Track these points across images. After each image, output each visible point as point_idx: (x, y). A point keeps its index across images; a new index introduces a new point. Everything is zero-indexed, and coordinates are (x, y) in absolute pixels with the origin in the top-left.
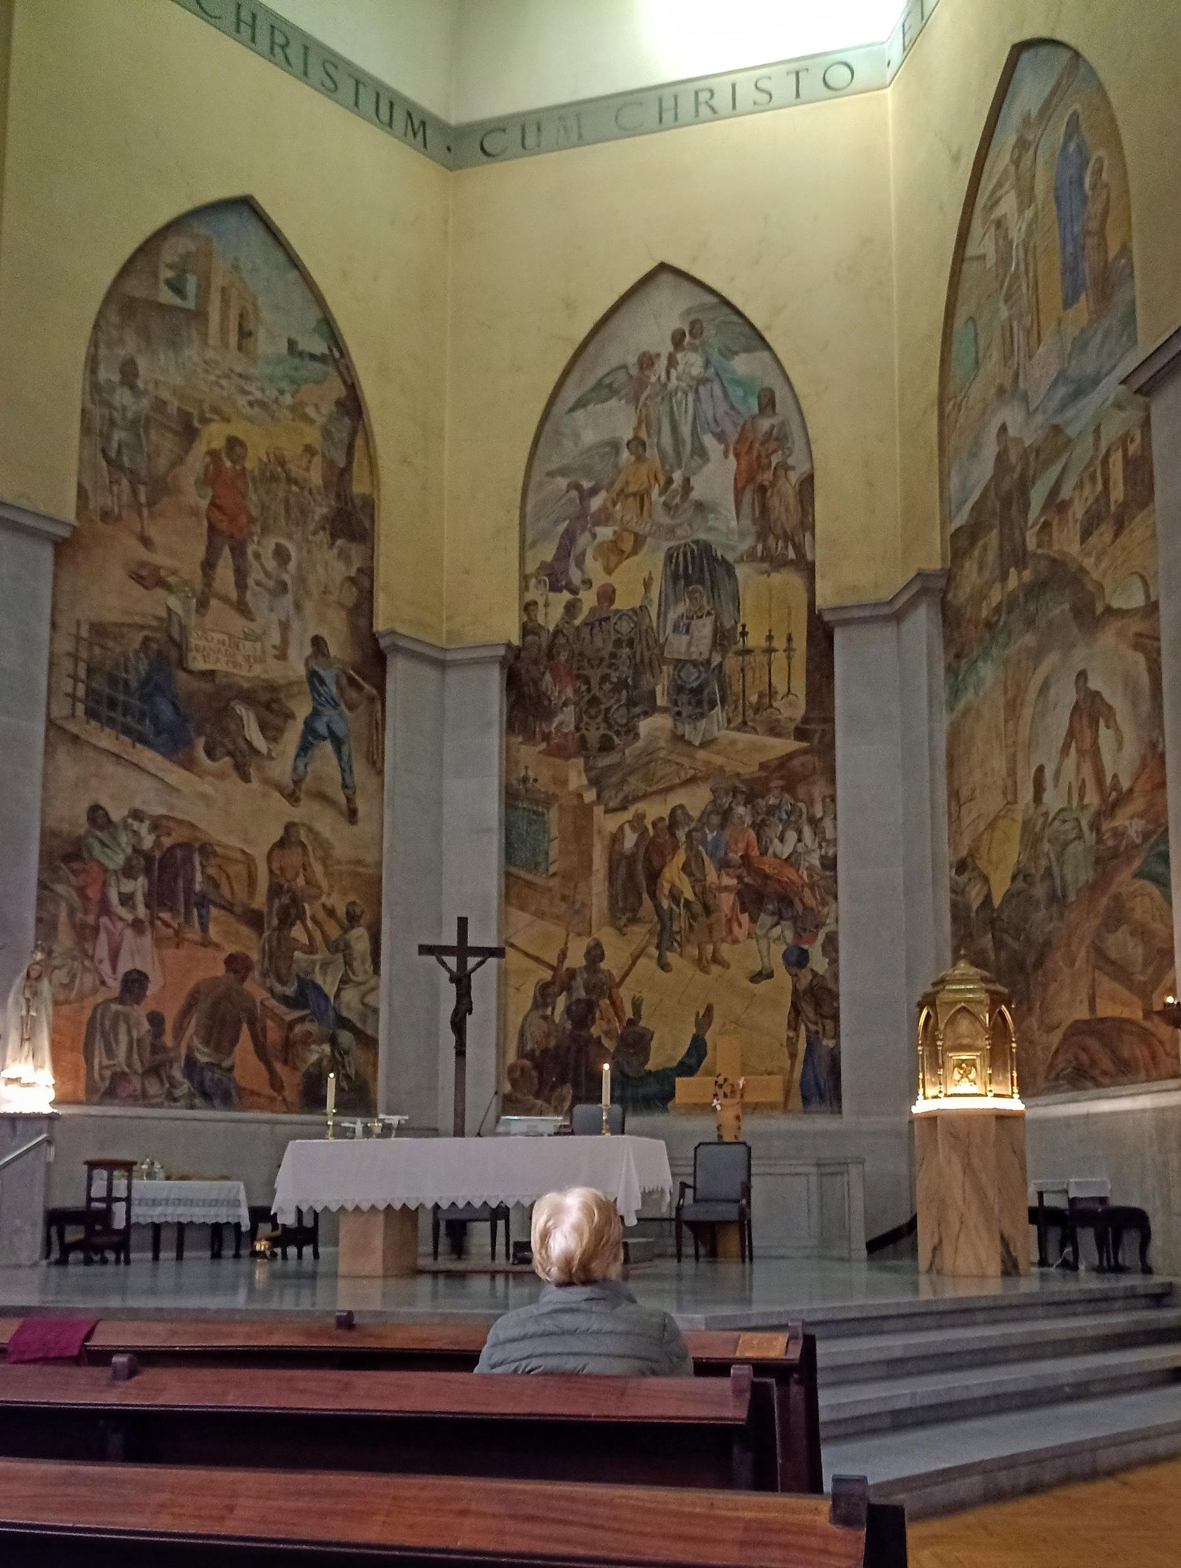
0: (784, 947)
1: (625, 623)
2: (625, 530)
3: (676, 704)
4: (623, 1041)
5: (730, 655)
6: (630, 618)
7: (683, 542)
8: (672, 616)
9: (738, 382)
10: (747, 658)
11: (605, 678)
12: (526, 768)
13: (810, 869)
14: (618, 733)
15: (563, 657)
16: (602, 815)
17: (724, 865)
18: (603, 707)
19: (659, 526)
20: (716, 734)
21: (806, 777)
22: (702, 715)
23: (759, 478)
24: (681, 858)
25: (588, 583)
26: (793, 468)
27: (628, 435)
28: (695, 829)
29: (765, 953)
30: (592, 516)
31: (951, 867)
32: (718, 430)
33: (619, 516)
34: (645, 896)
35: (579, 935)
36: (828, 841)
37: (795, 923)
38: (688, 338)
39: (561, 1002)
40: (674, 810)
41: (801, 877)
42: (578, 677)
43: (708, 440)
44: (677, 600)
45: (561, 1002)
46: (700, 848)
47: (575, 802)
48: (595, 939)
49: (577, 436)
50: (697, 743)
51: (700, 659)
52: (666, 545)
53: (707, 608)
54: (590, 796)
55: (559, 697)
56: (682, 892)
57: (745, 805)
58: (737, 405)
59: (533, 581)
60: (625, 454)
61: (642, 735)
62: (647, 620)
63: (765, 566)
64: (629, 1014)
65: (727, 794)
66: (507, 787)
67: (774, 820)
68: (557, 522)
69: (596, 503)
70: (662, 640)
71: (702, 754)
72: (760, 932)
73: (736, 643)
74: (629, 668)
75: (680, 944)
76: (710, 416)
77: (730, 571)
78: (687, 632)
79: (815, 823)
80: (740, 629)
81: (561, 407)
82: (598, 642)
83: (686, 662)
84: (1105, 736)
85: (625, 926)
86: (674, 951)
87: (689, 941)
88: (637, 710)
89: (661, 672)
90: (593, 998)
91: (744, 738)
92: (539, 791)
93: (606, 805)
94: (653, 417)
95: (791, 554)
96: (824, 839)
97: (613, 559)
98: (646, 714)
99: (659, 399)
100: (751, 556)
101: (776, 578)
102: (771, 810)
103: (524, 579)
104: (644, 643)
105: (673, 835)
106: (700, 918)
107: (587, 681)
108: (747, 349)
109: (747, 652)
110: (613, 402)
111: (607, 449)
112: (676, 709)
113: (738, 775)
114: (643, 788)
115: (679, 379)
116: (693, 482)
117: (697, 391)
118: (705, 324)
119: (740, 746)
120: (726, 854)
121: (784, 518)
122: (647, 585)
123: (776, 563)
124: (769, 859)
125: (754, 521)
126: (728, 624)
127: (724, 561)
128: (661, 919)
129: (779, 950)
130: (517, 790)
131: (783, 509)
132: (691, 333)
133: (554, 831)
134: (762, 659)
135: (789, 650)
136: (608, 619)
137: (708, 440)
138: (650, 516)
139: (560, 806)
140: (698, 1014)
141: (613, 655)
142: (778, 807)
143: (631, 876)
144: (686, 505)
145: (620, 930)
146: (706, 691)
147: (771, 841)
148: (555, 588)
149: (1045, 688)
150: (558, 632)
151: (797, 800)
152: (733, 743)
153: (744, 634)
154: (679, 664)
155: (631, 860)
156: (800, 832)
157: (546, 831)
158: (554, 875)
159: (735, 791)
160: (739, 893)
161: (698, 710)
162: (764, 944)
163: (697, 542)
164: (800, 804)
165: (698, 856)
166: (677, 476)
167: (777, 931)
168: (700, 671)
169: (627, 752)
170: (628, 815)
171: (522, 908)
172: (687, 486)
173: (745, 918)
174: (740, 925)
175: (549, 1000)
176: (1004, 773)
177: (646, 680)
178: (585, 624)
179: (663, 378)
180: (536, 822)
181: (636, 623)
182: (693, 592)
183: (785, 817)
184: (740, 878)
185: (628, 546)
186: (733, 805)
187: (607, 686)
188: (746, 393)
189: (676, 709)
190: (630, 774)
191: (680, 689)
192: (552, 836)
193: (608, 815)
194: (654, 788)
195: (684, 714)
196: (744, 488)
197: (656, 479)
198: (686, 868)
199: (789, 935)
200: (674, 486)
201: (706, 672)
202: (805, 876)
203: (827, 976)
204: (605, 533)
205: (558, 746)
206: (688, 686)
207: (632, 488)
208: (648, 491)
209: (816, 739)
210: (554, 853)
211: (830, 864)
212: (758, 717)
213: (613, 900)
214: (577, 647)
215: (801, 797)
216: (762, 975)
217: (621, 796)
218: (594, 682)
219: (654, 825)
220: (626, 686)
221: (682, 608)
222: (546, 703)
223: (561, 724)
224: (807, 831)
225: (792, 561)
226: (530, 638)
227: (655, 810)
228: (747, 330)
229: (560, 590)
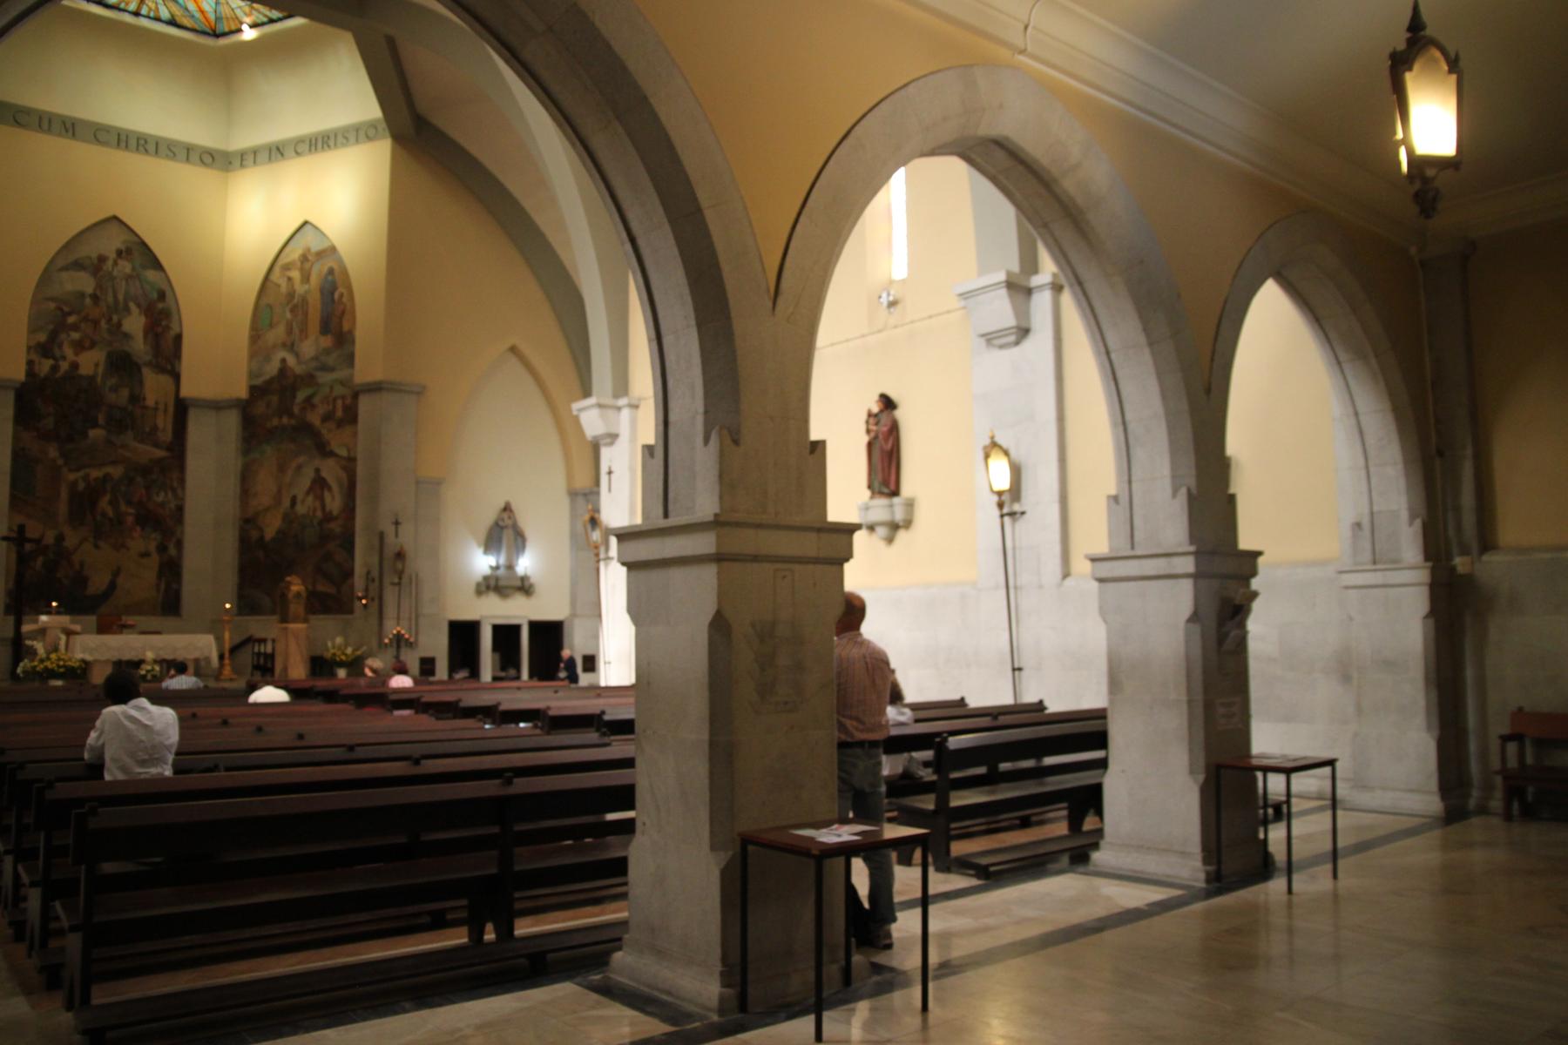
17: (129, 503)
24: (107, 497)
25: (64, 358)
27: (89, 290)
43: (132, 305)
54: (60, 462)
60: (88, 301)
69: (71, 319)
79: (174, 490)
84: (327, 494)
91: (142, 447)
100: (149, 364)
103: (29, 348)
109: (145, 407)
110: (82, 274)
122: (97, 365)
123: (160, 369)
129: (152, 546)
135: (166, 411)
149: (299, 467)
166: (115, 318)
167: (153, 536)
170: (81, 473)
172: (119, 324)
173: (138, 528)
179: (110, 269)
185: (87, 344)
198: (111, 503)
204: (75, 336)
211: (180, 509)
216: (146, 555)
224: (170, 494)
227: (96, 474)
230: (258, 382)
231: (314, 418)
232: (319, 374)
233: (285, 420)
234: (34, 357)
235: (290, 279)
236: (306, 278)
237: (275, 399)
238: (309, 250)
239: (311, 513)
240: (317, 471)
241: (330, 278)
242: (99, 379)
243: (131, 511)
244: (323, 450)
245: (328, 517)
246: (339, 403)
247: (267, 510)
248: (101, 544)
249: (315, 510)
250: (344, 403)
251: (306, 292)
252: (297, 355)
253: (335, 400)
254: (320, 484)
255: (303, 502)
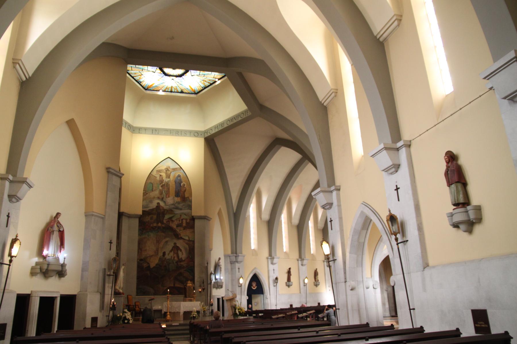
31: (138, 259)
149: (167, 242)
176: (155, 249)
230: (147, 209)
231: (174, 225)
232: (175, 210)
233: (160, 224)
235: (161, 175)
236: (168, 176)
237: (155, 217)
238: (170, 167)
239: (172, 258)
240: (175, 244)
241: (179, 178)
244: (177, 236)
245: (180, 260)
246: (184, 221)
247: (151, 256)
249: (174, 257)
250: (186, 221)
251: (168, 181)
252: (165, 202)
253: (182, 220)
254: (176, 248)
255: (169, 254)
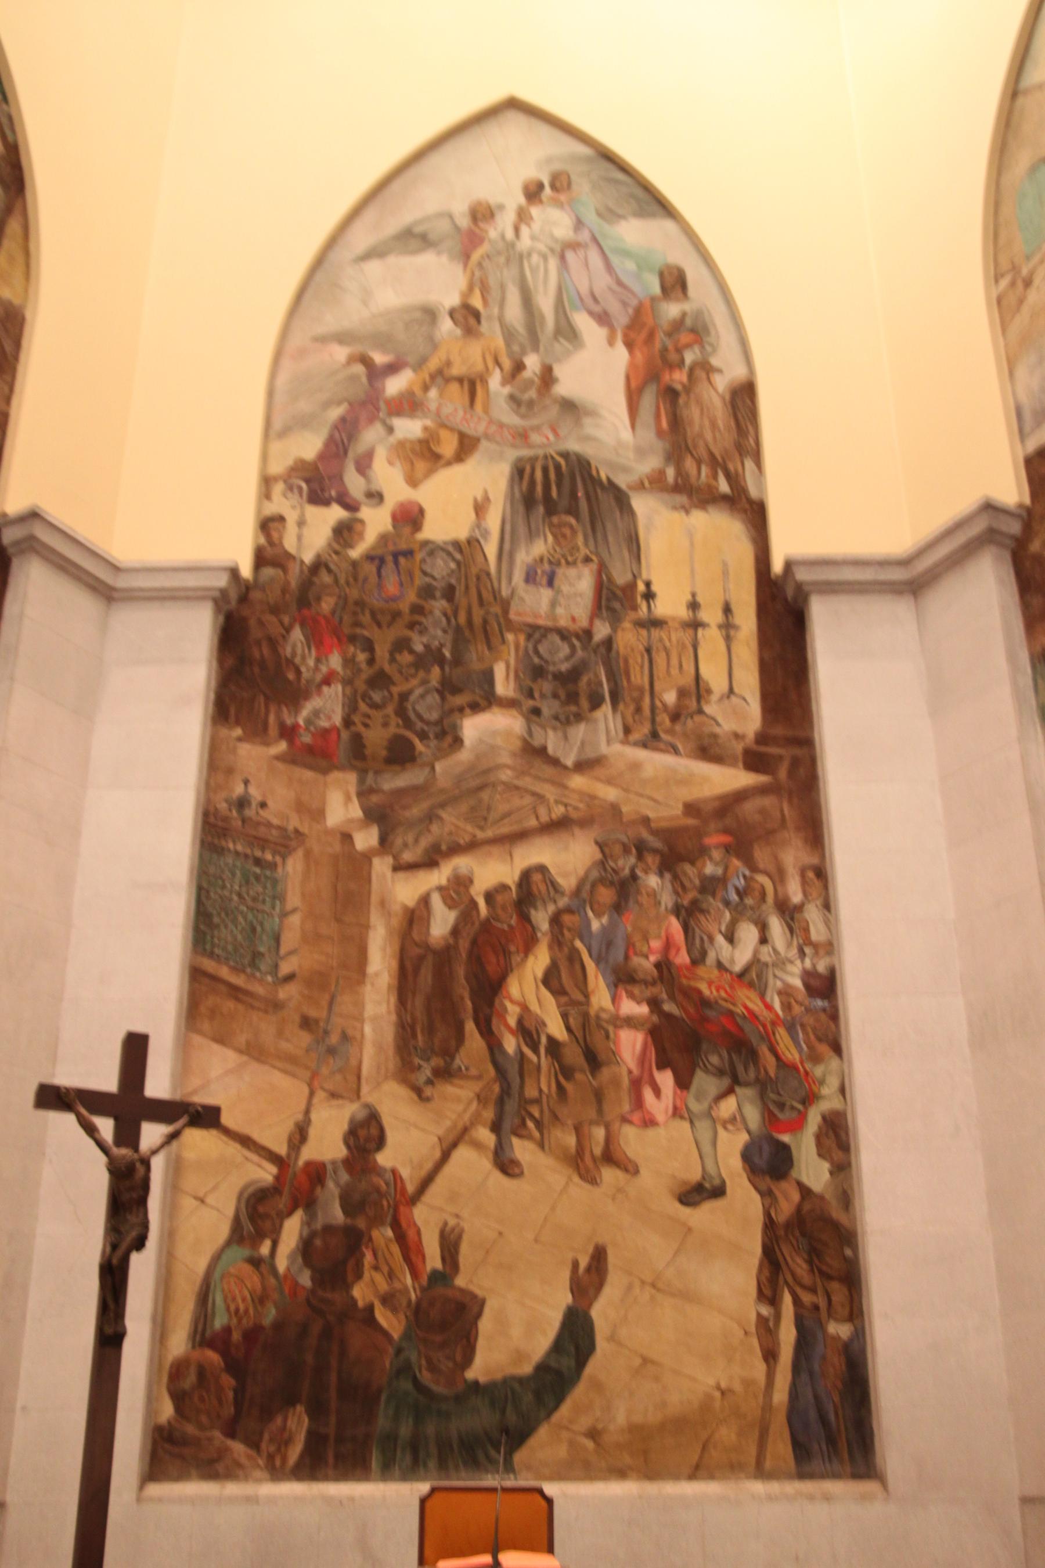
0: (744, 1138)
1: (440, 562)
2: (443, 425)
3: (530, 695)
4: (418, 1314)
5: (627, 625)
6: (449, 554)
7: (541, 452)
8: (526, 555)
9: (626, 253)
10: (656, 633)
11: (401, 645)
12: (246, 782)
13: (786, 993)
14: (423, 736)
15: (327, 605)
16: (389, 873)
18: (395, 690)
19: (501, 426)
20: (604, 749)
21: (772, 832)
22: (579, 717)
23: (666, 377)
24: (539, 961)
25: (376, 497)
26: (719, 371)
27: (453, 300)
28: (569, 910)
29: (707, 1148)
30: (388, 403)
32: (597, 309)
33: (433, 406)
34: (470, 1026)
35: (334, 1095)
36: (815, 946)
37: (762, 1096)
38: (547, 190)
39: (292, 1229)
40: (526, 876)
41: (769, 1007)
42: (353, 639)
43: (583, 322)
44: (532, 535)
45: (292, 1229)
46: (578, 944)
47: (337, 847)
48: (367, 1106)
49: (366, 296)
50: (569, 762)
51: (573, 627)
52: (512, 454)
53: (584, 551)
54: (366, 839)
55: (317, 669)
56: (544, 1024)
57: (661, 875)
58: (625, 279)
59: (278, 488)
60: (446, 325)
61: (467, 742)
62: (480, 559)
63: (683, 499)
64: (433, 1260)
65: (626, 850)
66: (206, 814)
67: (714, 904)
68: (327, 405)
69: (395, 385)
70: (505, 592)
71: (577, 781)
72: (695, 1106)
73: (635, 608)
74: (445, 631)
75: (539, 1124)
76: (584, 290)
77: (621, 500)
78: (550, 583)
79: (789, 912)
80: (641, 587)
81: (344, 253)
82: (391, 586)
83: (546, 631)
85: (430, 1082)
86: (529, 1137)
87: (555, 1117)
88: (459, 700)
89: (504, 641)
90: (361, 1223)
92: (269, 825)
93: (395, 858)
94: (492, 282)
95: (724, 487)
96: (808, 942)
97: (421, 466)
98: (476, 708)
99: (502, 260)
100: (656, 483)
101: (700, 519)
102: (710, 886)
103: (267, 482)
104: (473, 591)
105: (525, 918)
106: (579, 1076)
107: (369, 646)
108: (641, 213)
109: (657, 623)
110: (428, 259)
111: (418, 315)
112: (531, 703)
113: (646, 821)
114: (470, 829)
115: (533, 238)
116: (558, 371)
117: (562, 258)
118: (573, 178)
119: (648, 772)
120: (627, 957)
121: (709, 436)
122: (480, 508)
124: (708, 971)
125: (660, 433)
126: (621, 577)
127: (612, 486)
128: (501, 1072)
130: (226, 819)
131: (707, 423)
132: (553, 187)
133: (294, 899)
134: (677, 636)
135: (728, 627)
136: (409, 553)
137: (583, 322)
138: (486, 410)
139: (308, 854)
140: (575, 1265)
141: (417, 610)
142: (722, 881)
143: (443, 989)
144: (548, 401)
145: (418, 1091)
146: (584, 679)
147: (711, 939)
148: (318, 498)
150: (318, 565)
151: (754, 869)
152: (635, 766)
153: (649, 596)
154: (535, 632)
155: (444, 956)
156: (763, 928)
157: (279, 897)
158: (290, 978)
159: (641, 849)
160: (655, 1034)
161: (573, 708)
162: (704, 1127)
163: (566, 455)
164: (763, 879)
165: (574, 957)
166: (532, 363)
167: (728, 1106)
168: (573, 648)
169: (438, 767)
170: (440, 876)
171: (221, 1039)
172: (548, 377)
173: (666, 1079)
174: (657, 1092)
175: (267, 1225)
177: (475, 656)
178: (369, 557)
179: (510, 234)
180: (257, 878)
181: (458, 563)
182: (560, 525)
183: (734, 897)
184: (654, 1004)
185: (448, 446)
186: (639, 872)
187: (406, 658)
188: (639, 267)
189: (531, 703)
190: (443, 805)
191: (538, 672)
192: (289, 906)
193: (401, 875)
194: (489, 833)
195: (546, 711)
196: (640, 390)
197: (497, 363)
198: (550, 980)
199: (753, 1115)
200: (527, 374)
201: (584, 648)
202: (777, 1005)
203: (827, 1196)
204: (410, 428)
205: (310, 750)
206: (551, 668)
207: (456, 371)
208: (483, 379)
209: (783, 773)
210: (290, 939)
212: (678, 728)
213: (405, 1032)
214: (354, 593)
215: (761, 866)
217: (424, 842)
218: (382, 652)
219: (489, 897)
220: (441, 661)
221: (540, 548)
222: (291, 676)
223: (316, 713)
224: (776, 927)
225: (725, 498)
226: (268, 572)
228: (640, 193)
229: (326, 502)
234: (281, 504)
242: (491, 549)
243: (633, 1008)
248: (522, 1150)
